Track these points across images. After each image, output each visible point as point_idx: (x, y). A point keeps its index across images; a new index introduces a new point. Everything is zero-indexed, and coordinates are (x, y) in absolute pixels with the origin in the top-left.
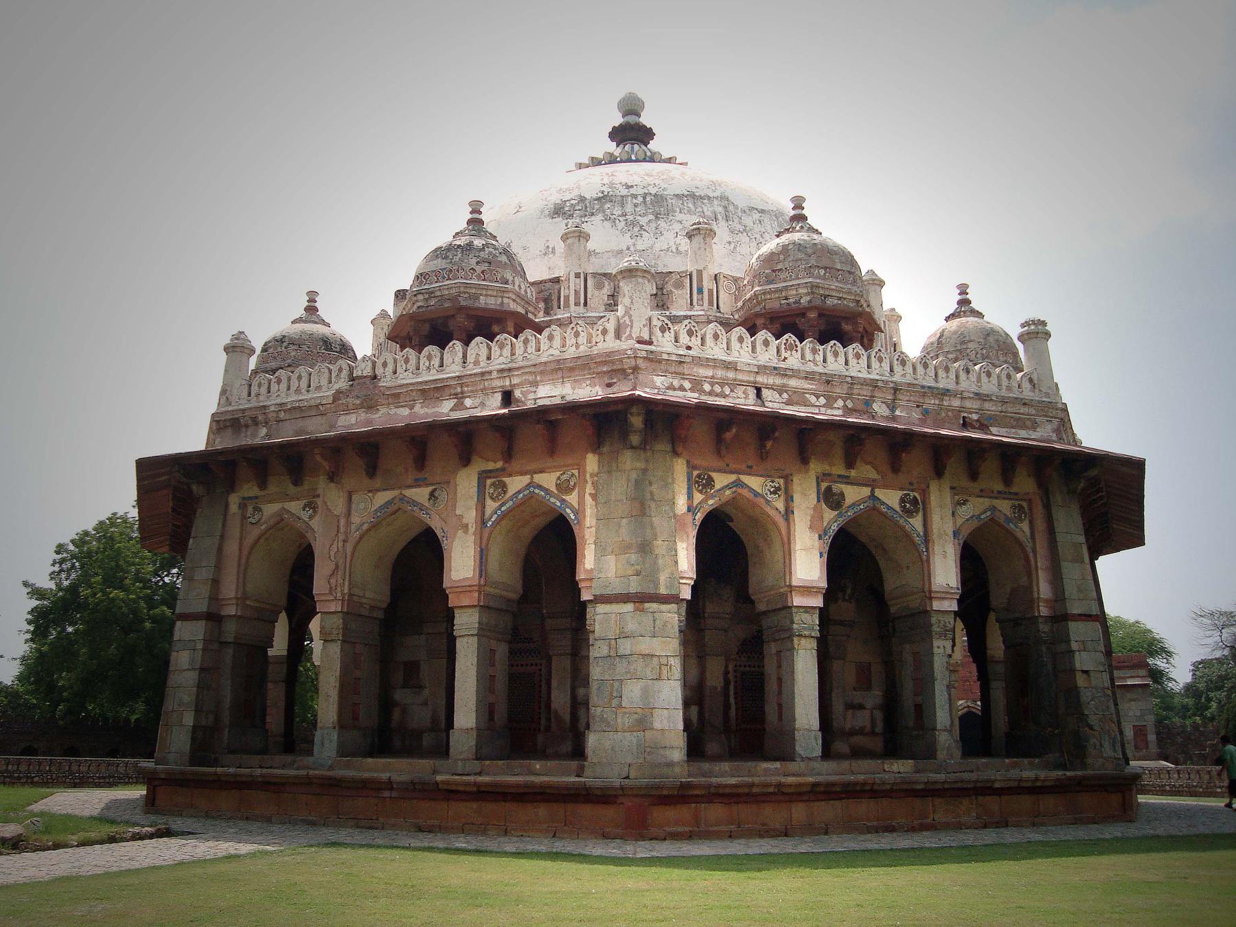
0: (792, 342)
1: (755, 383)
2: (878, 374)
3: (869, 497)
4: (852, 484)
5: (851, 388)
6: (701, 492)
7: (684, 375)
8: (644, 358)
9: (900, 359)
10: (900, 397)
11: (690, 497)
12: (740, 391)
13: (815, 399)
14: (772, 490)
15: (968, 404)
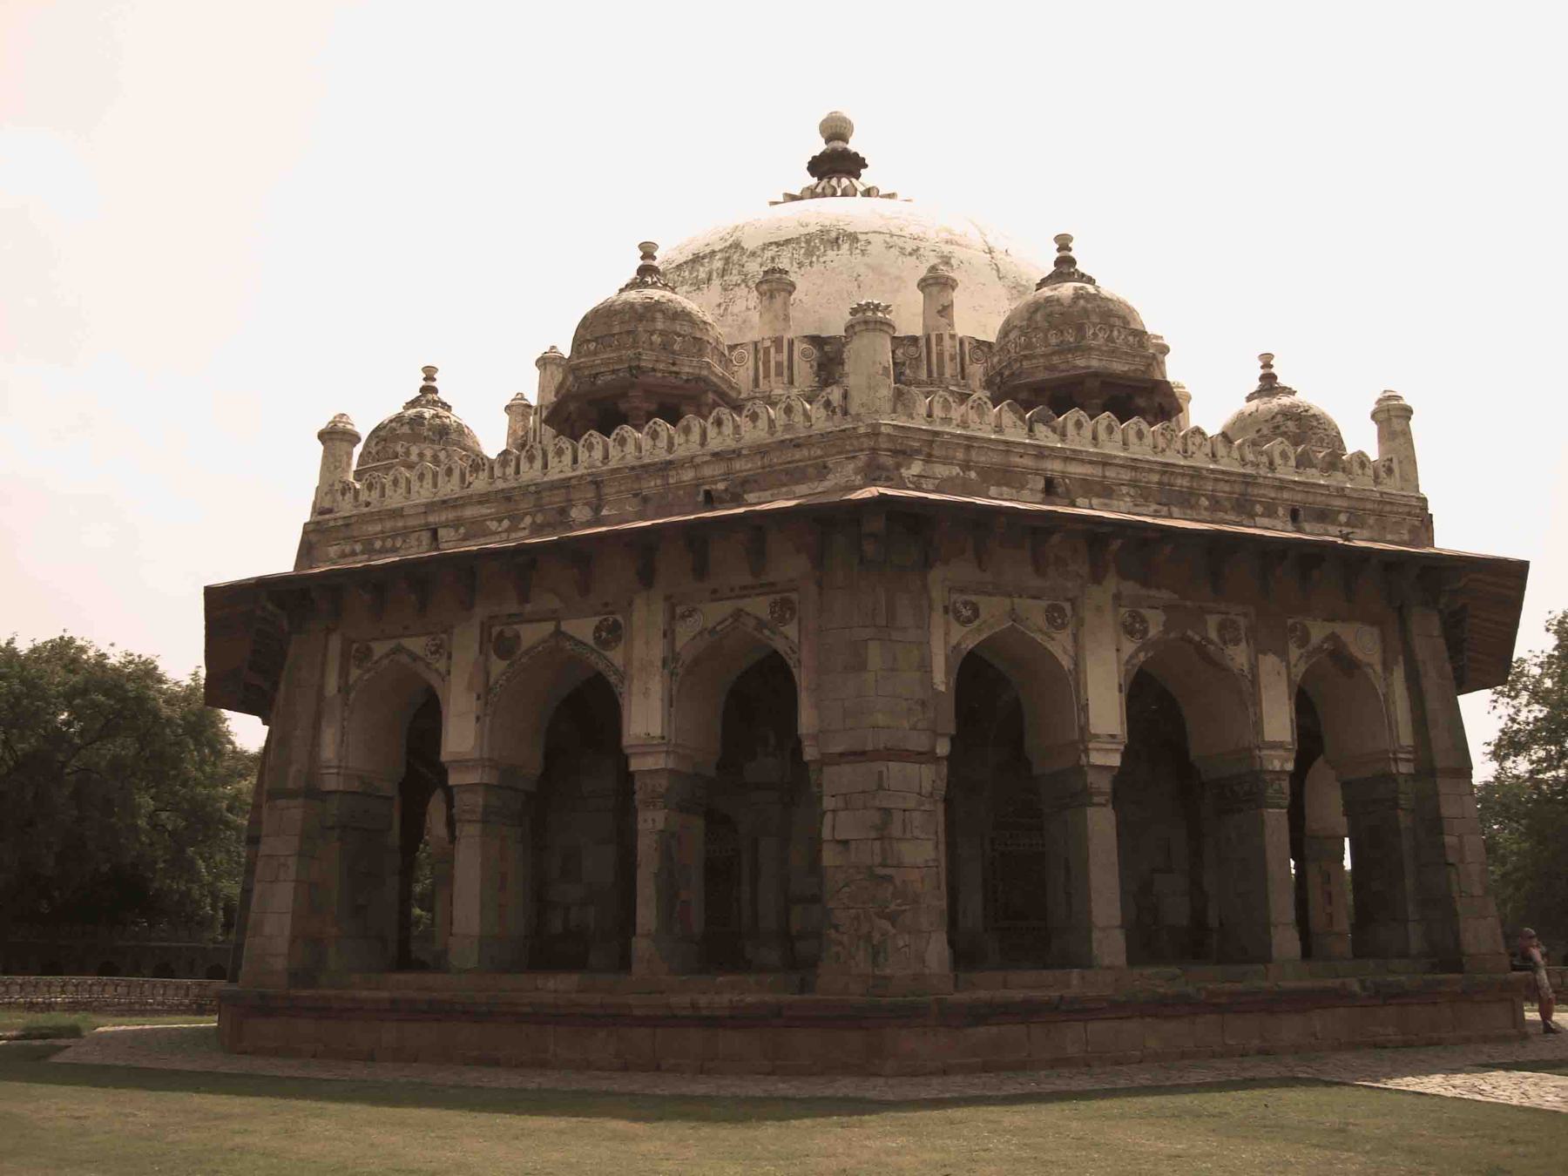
0: (480, 461)
1: (427, 524)
2: (585, 468)
3: (551, 635)
4: (531, 621)
5: (541, 498)
6: (359, 667)
7: (355, 537)
8: (313, 531)
9: (619, 437)
10: (606, 490)
11: (344, 673)
12: (413, 540)
13: (493, 525)
14: (433, 649)
15: (707, 472)
